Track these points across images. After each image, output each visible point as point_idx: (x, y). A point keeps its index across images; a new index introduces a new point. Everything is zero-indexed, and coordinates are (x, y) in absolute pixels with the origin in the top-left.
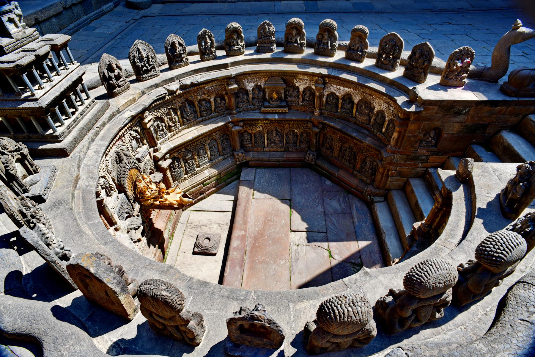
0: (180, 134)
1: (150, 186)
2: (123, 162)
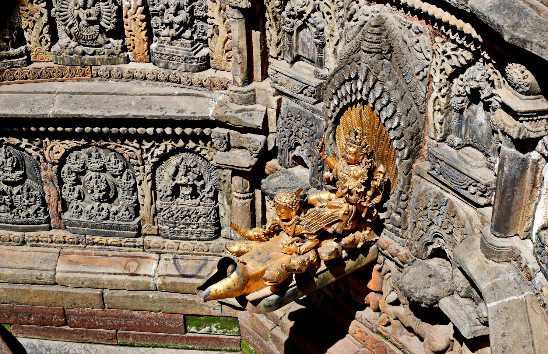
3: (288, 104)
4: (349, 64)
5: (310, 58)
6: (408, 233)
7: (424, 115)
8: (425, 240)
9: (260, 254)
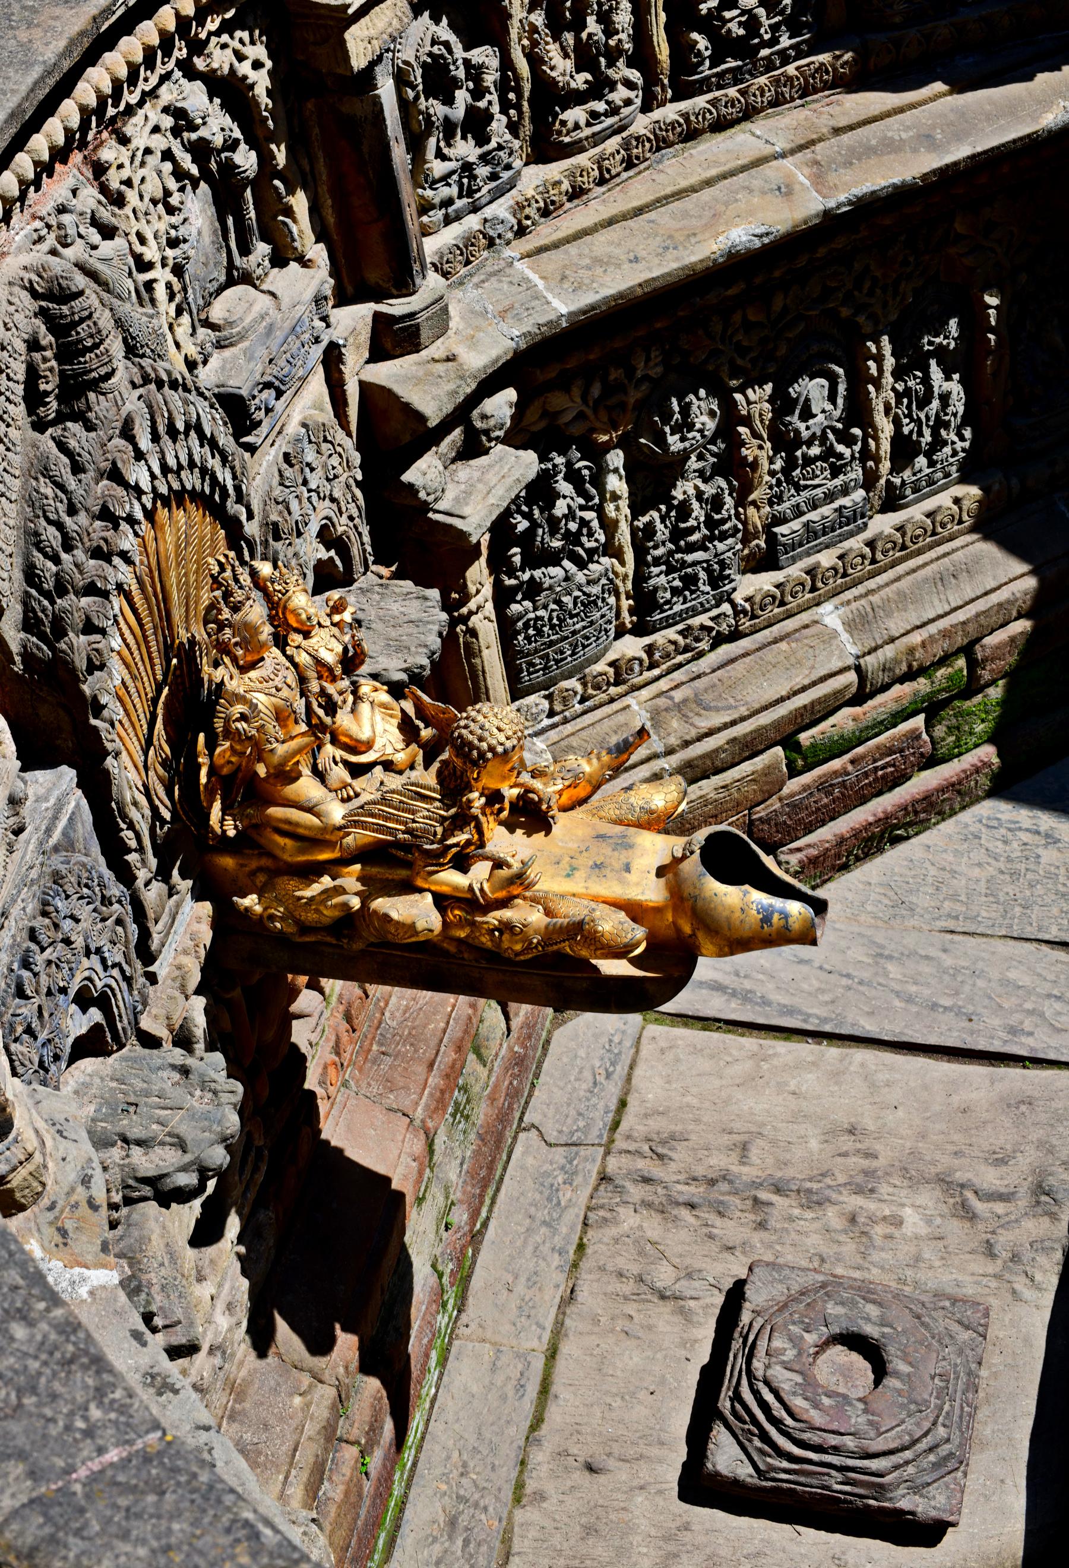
0: (638, 188)
1: (343, 719)
2: (100, 406)
9: (597, 866)
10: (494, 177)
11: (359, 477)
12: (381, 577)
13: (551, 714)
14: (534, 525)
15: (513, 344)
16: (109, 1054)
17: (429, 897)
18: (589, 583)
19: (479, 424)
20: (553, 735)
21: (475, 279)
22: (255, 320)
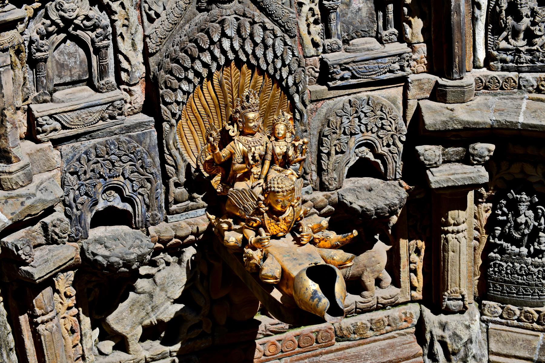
3: (74, 148)
4: (202, 30)
5: (75, 78)
6: (311, 176)
7: (297, 37)
8: (345, 161)
10: (532, 61)
11: (404, 139)
12: (401, 185)
13: (501, 317)
14: (508, 221)
15: (491, 122)
16: (133, 228)
17: (241, 236)
18: (532, 264)
19: (471, 150)
20: (498, 327)
21: (501, 97)
22: (364, 49)
